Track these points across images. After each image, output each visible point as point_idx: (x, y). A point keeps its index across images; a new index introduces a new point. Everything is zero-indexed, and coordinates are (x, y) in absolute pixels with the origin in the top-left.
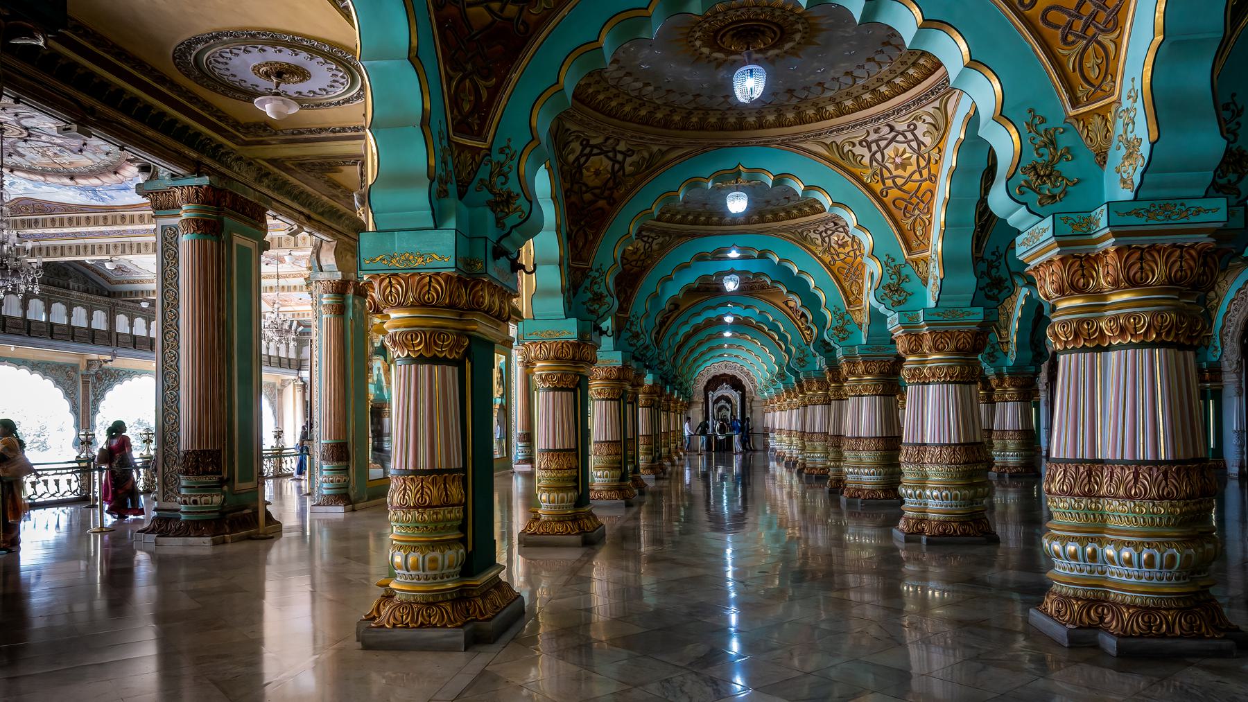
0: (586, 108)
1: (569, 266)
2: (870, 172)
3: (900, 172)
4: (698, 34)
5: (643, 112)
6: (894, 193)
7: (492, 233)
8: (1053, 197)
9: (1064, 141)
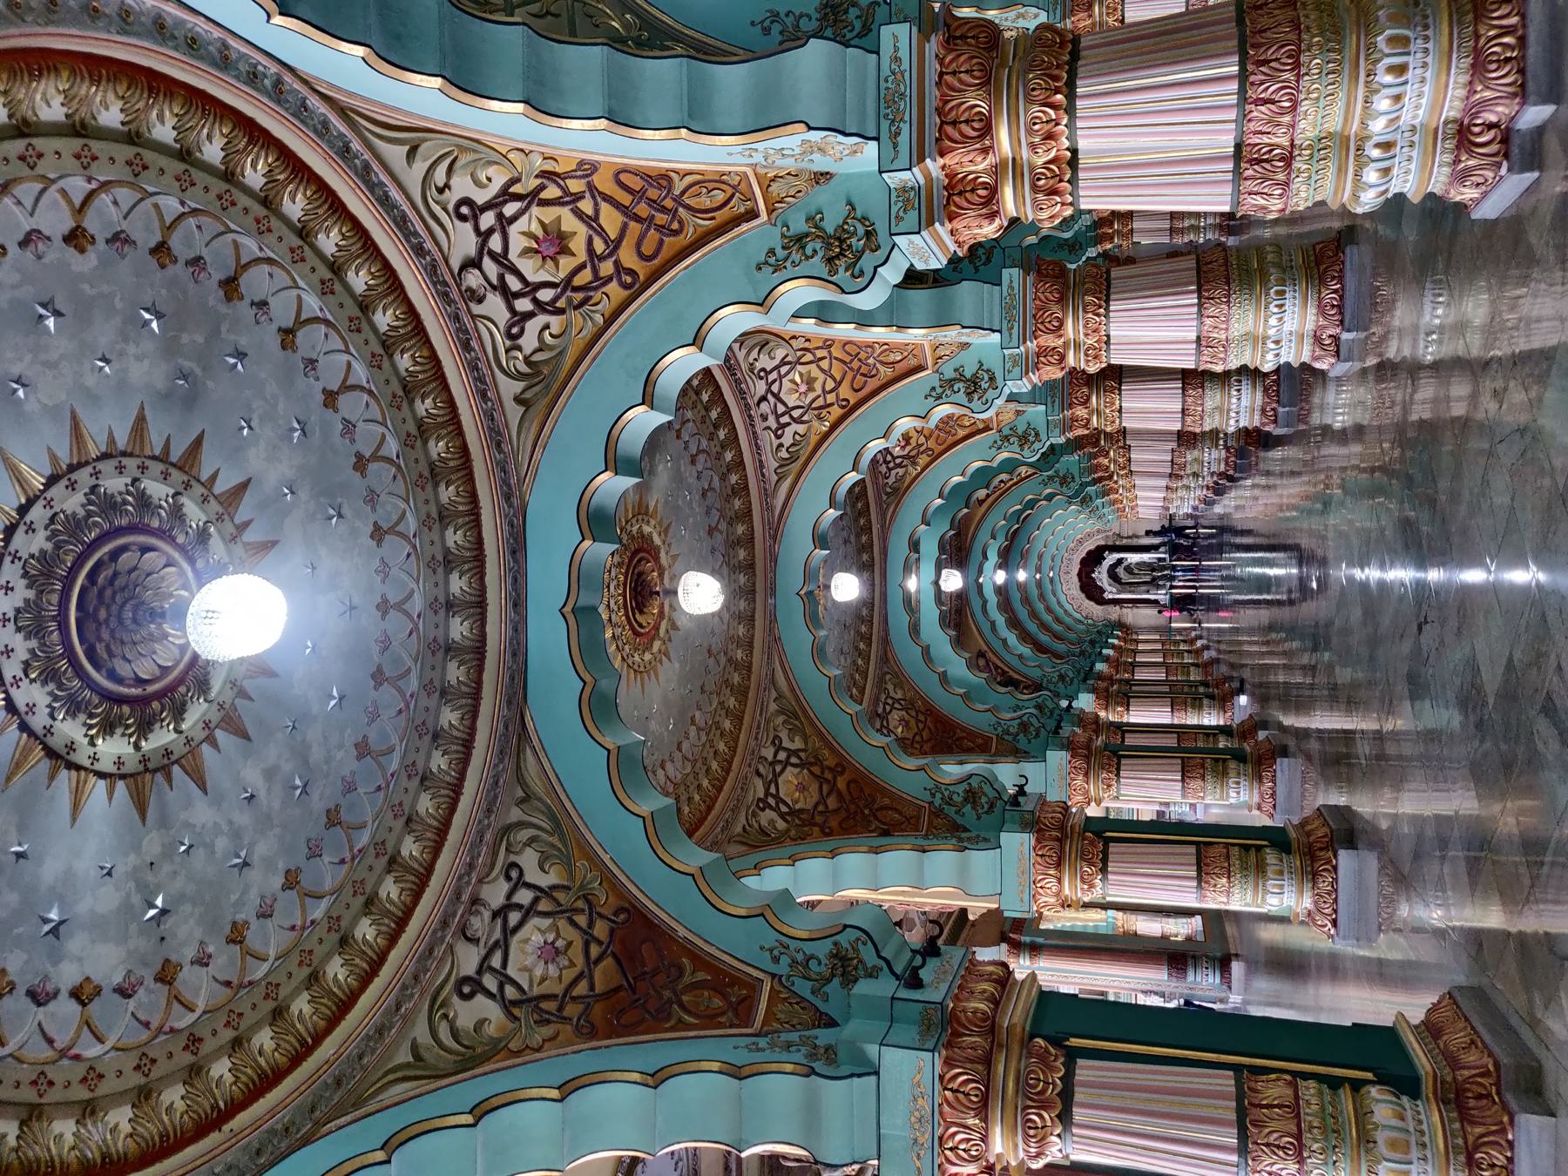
0: (718, 806)
1: (926, 837)
2: (815, 423)
3: (818, 386)
4: (637, 658)
5: (727, 725)
6: (845, 391)
7: (884, 987)
8: (868, 234)
9: (799, 225)
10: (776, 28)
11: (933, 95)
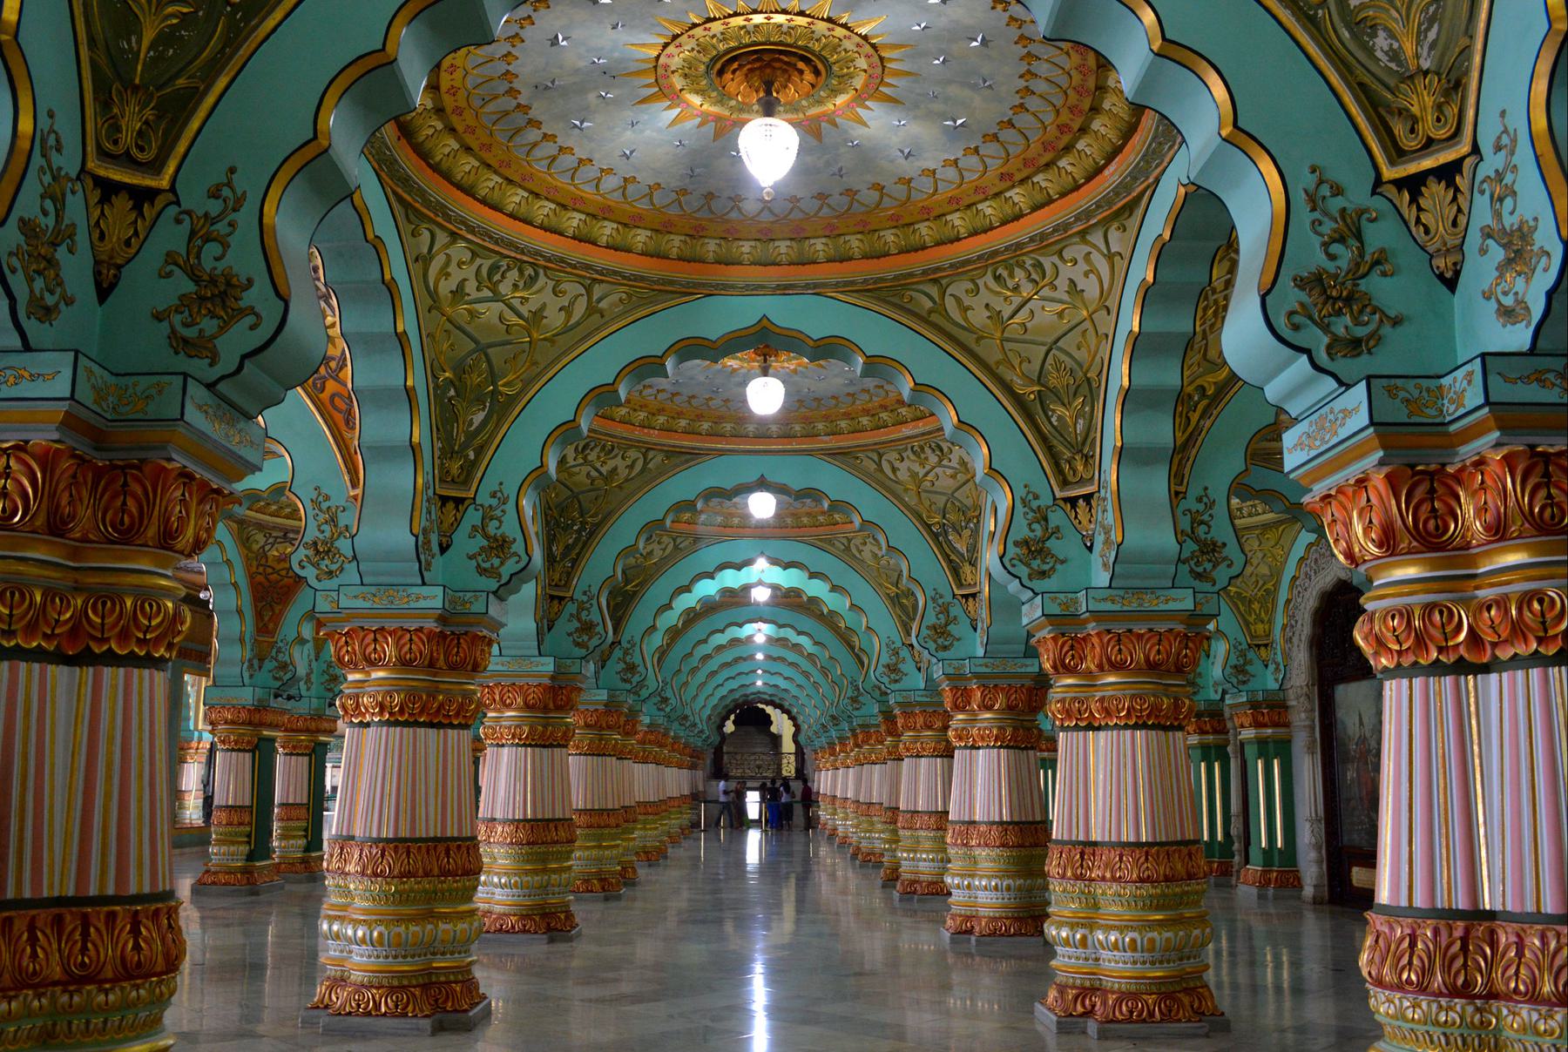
8: (331, 573)
10: (494, 502)
11: (391, 625)
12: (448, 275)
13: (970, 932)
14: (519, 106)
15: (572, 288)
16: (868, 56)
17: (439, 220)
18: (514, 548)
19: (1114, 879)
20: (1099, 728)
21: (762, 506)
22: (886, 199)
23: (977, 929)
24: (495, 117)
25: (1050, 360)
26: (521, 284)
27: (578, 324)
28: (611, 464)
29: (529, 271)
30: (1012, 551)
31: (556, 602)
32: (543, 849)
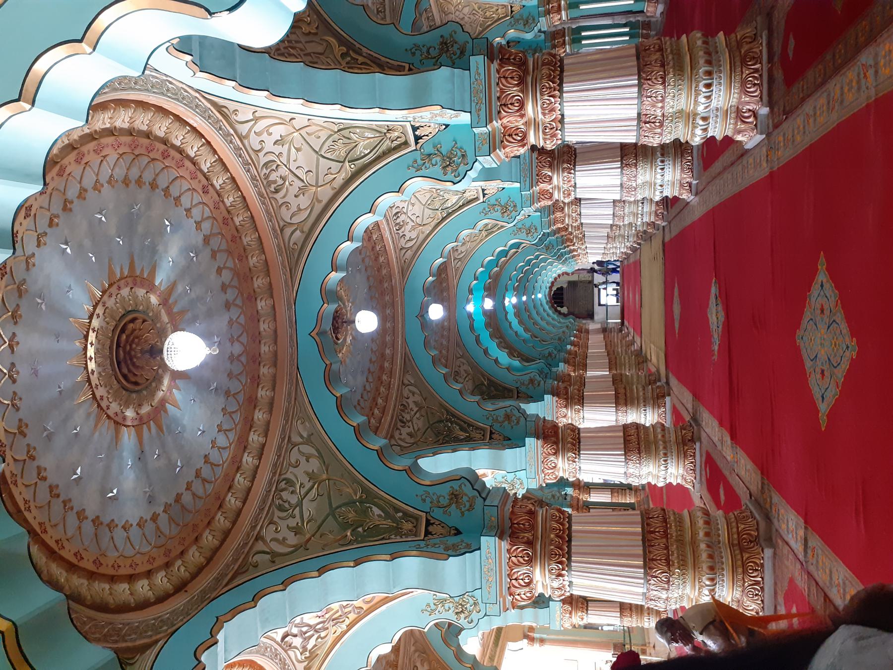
11: (505, 570)
12: (284, 539)
13: (690, 185)
14: (165, 511)
15: (294, 455)
16: (119, 288)
17: (246, 552)
18: (456, 487)
19: (662, 101)
20: (563, 115)
21: (436, 312)
22: (228, 265)
23: (688, 180)
24: (173, 526)
25: (328, 155)
26: (291, 489)
27: (318, 450)
28: (412, 405)
29: (283, 485)
30: (450, 176)
31: (493, 436)
32: (642, 444)
